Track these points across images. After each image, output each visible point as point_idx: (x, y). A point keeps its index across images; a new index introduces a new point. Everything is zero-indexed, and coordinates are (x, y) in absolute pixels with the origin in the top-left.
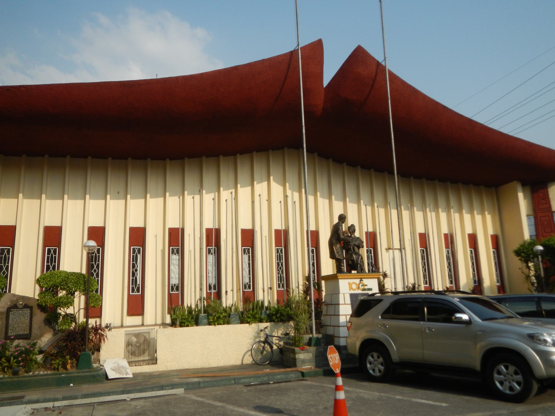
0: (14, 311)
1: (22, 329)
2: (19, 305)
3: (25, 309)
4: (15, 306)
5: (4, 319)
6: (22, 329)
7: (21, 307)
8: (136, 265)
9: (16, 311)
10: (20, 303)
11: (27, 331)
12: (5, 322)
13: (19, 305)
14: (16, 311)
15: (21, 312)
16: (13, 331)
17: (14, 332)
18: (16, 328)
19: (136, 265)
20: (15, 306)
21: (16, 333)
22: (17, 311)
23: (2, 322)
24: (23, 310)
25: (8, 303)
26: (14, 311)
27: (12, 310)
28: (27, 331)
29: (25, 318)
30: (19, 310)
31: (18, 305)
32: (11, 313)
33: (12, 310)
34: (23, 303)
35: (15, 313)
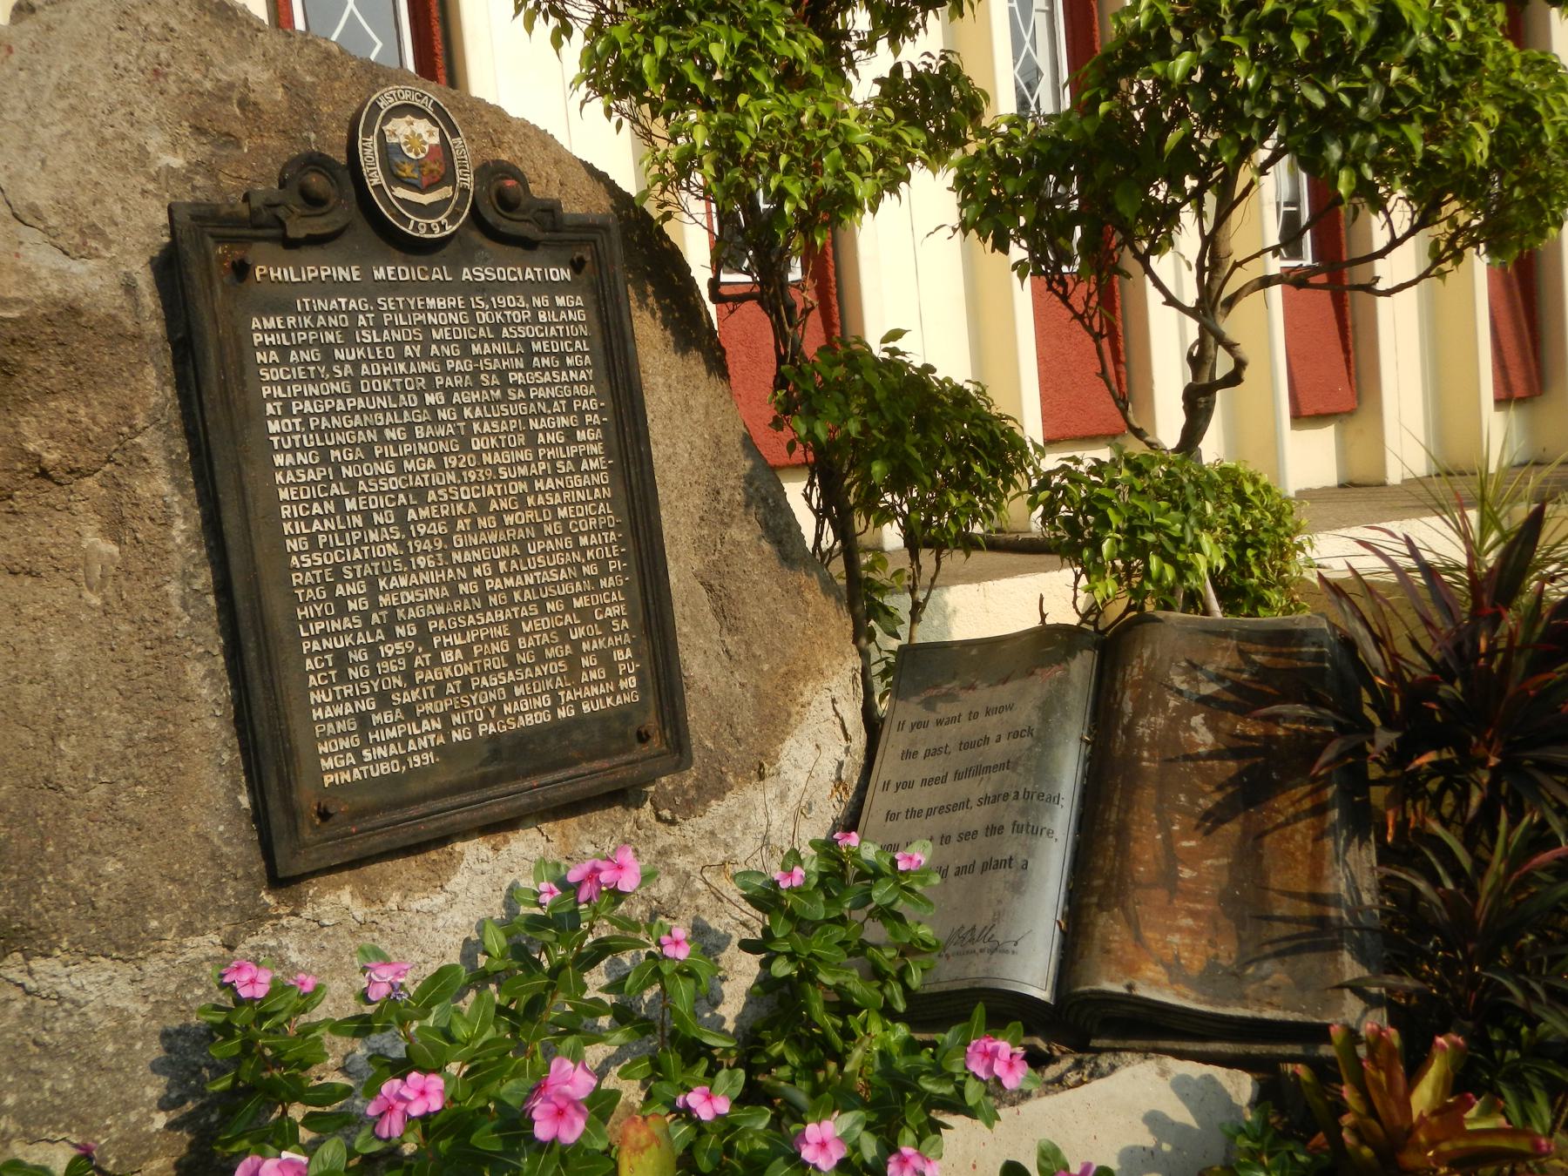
0: (332, 288)
1: (537, 628)
2: (395, 178)
3: (503, 274)
4: (313, 201)
5: (157, 459)
6: (537, 628)
7: (439, 228)
8: (1027, 30)
9: (347, 288)
10: (401, 130)
11: (613, 674)
12: (183, 529)
13: (395, 178)
14: (347, 288)
15: (442, 311)
16: (384, 700)
17: (409, 711)
18: (424, 638)
19: (1027, 30)
20: (313, 201)
21: (448, 727)
22: (369, 289)
23: (115, 527)
24: (487, 289)
25: (155, 141)
26: (332, 288)
27: (289, 274)
28: (613, 674)
29: (531, 440)
30: (408, 273)
31: (375, 177)
32: (264, 328)
33: (289, 274)
34: (460, 146)
35: (349, 336)
